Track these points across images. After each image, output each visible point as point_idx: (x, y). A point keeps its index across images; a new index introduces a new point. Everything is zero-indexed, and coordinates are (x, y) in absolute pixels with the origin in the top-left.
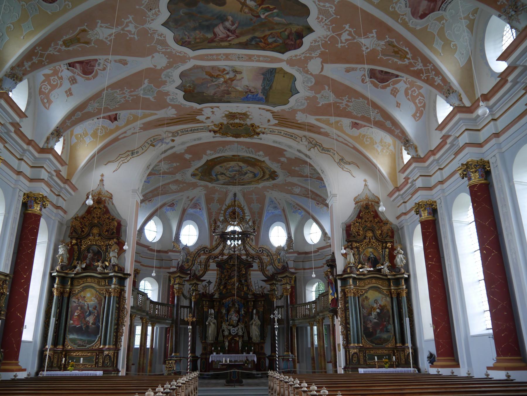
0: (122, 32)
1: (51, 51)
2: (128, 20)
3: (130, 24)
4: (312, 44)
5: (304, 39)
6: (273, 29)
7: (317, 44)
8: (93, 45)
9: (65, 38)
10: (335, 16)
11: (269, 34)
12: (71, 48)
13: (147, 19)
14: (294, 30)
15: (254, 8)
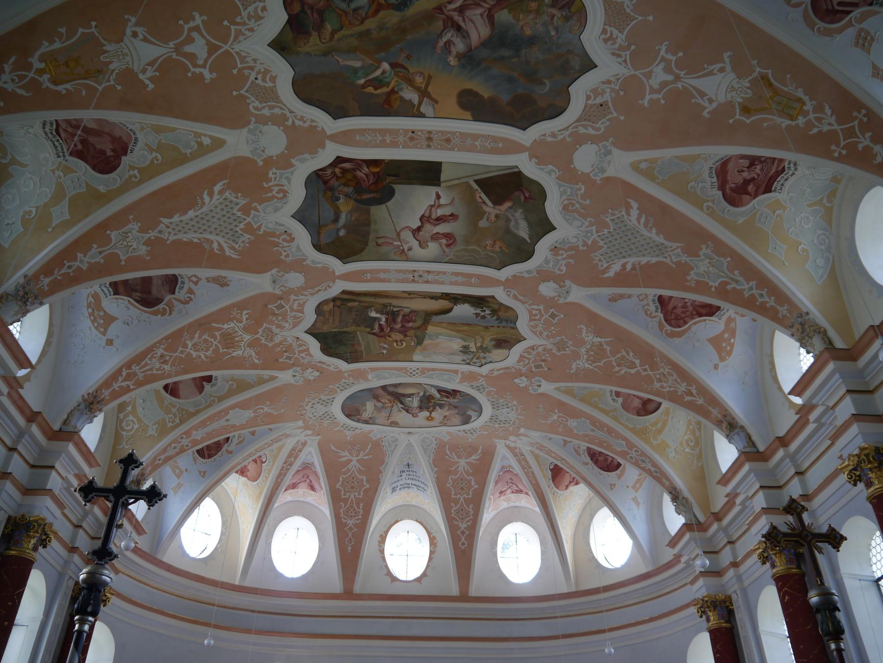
0: (682, 73)
1: (830, 124)
2: (655, 96)
3: (656, 87)
4: (261, 4)
5: (285, 17)
6: (360, 35)
7: (251, 9)
8: (758, 69)
9: (785, 122)
10: (242, 92)
11: (366, 21)
12: (800, 93)
13: (617, 88)
14: (314, 39)
15: (404, 85)
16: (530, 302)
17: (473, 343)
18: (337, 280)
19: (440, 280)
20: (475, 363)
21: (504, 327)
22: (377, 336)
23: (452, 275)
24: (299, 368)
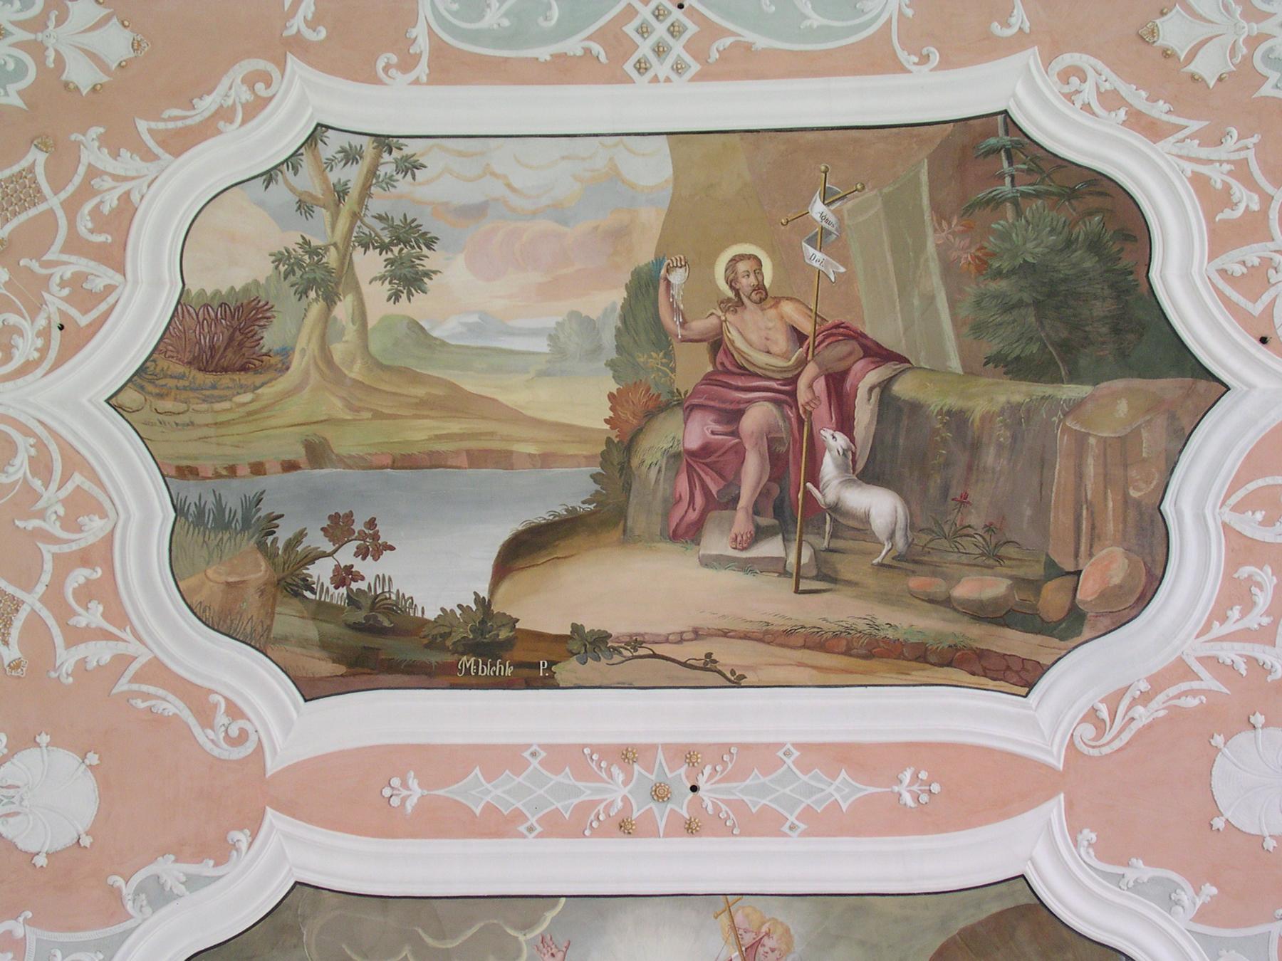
16: (123, 686)
17: (372, 321)
18: (1057, 760)
19: (566, 778)
20: (351, 156)
21: (232, 471)
22: (858, 337)
23: (518, 816)
24: (1267, 90)
